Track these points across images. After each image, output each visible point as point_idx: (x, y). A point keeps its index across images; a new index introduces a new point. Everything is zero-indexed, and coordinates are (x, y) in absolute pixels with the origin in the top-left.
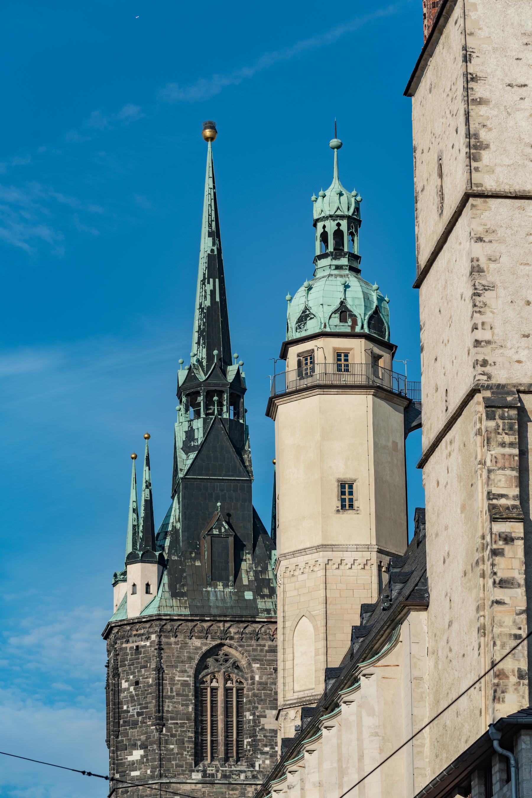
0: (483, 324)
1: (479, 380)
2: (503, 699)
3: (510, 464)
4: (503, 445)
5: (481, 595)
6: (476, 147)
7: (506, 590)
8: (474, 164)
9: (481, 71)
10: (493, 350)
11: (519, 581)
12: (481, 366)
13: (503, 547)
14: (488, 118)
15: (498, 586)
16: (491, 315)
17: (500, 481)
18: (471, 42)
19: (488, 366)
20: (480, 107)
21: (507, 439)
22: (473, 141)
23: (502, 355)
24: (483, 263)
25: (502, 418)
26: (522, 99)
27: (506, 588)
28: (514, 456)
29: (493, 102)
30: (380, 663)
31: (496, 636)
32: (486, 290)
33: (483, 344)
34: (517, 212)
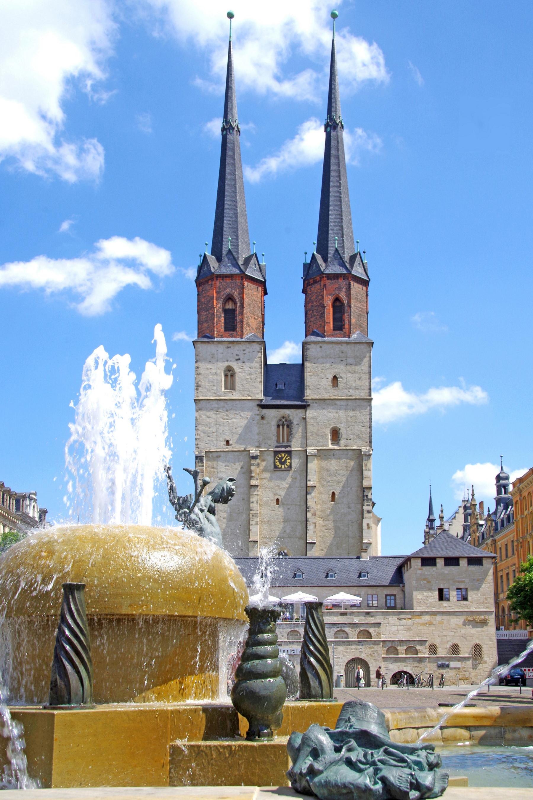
4: (200, 466)
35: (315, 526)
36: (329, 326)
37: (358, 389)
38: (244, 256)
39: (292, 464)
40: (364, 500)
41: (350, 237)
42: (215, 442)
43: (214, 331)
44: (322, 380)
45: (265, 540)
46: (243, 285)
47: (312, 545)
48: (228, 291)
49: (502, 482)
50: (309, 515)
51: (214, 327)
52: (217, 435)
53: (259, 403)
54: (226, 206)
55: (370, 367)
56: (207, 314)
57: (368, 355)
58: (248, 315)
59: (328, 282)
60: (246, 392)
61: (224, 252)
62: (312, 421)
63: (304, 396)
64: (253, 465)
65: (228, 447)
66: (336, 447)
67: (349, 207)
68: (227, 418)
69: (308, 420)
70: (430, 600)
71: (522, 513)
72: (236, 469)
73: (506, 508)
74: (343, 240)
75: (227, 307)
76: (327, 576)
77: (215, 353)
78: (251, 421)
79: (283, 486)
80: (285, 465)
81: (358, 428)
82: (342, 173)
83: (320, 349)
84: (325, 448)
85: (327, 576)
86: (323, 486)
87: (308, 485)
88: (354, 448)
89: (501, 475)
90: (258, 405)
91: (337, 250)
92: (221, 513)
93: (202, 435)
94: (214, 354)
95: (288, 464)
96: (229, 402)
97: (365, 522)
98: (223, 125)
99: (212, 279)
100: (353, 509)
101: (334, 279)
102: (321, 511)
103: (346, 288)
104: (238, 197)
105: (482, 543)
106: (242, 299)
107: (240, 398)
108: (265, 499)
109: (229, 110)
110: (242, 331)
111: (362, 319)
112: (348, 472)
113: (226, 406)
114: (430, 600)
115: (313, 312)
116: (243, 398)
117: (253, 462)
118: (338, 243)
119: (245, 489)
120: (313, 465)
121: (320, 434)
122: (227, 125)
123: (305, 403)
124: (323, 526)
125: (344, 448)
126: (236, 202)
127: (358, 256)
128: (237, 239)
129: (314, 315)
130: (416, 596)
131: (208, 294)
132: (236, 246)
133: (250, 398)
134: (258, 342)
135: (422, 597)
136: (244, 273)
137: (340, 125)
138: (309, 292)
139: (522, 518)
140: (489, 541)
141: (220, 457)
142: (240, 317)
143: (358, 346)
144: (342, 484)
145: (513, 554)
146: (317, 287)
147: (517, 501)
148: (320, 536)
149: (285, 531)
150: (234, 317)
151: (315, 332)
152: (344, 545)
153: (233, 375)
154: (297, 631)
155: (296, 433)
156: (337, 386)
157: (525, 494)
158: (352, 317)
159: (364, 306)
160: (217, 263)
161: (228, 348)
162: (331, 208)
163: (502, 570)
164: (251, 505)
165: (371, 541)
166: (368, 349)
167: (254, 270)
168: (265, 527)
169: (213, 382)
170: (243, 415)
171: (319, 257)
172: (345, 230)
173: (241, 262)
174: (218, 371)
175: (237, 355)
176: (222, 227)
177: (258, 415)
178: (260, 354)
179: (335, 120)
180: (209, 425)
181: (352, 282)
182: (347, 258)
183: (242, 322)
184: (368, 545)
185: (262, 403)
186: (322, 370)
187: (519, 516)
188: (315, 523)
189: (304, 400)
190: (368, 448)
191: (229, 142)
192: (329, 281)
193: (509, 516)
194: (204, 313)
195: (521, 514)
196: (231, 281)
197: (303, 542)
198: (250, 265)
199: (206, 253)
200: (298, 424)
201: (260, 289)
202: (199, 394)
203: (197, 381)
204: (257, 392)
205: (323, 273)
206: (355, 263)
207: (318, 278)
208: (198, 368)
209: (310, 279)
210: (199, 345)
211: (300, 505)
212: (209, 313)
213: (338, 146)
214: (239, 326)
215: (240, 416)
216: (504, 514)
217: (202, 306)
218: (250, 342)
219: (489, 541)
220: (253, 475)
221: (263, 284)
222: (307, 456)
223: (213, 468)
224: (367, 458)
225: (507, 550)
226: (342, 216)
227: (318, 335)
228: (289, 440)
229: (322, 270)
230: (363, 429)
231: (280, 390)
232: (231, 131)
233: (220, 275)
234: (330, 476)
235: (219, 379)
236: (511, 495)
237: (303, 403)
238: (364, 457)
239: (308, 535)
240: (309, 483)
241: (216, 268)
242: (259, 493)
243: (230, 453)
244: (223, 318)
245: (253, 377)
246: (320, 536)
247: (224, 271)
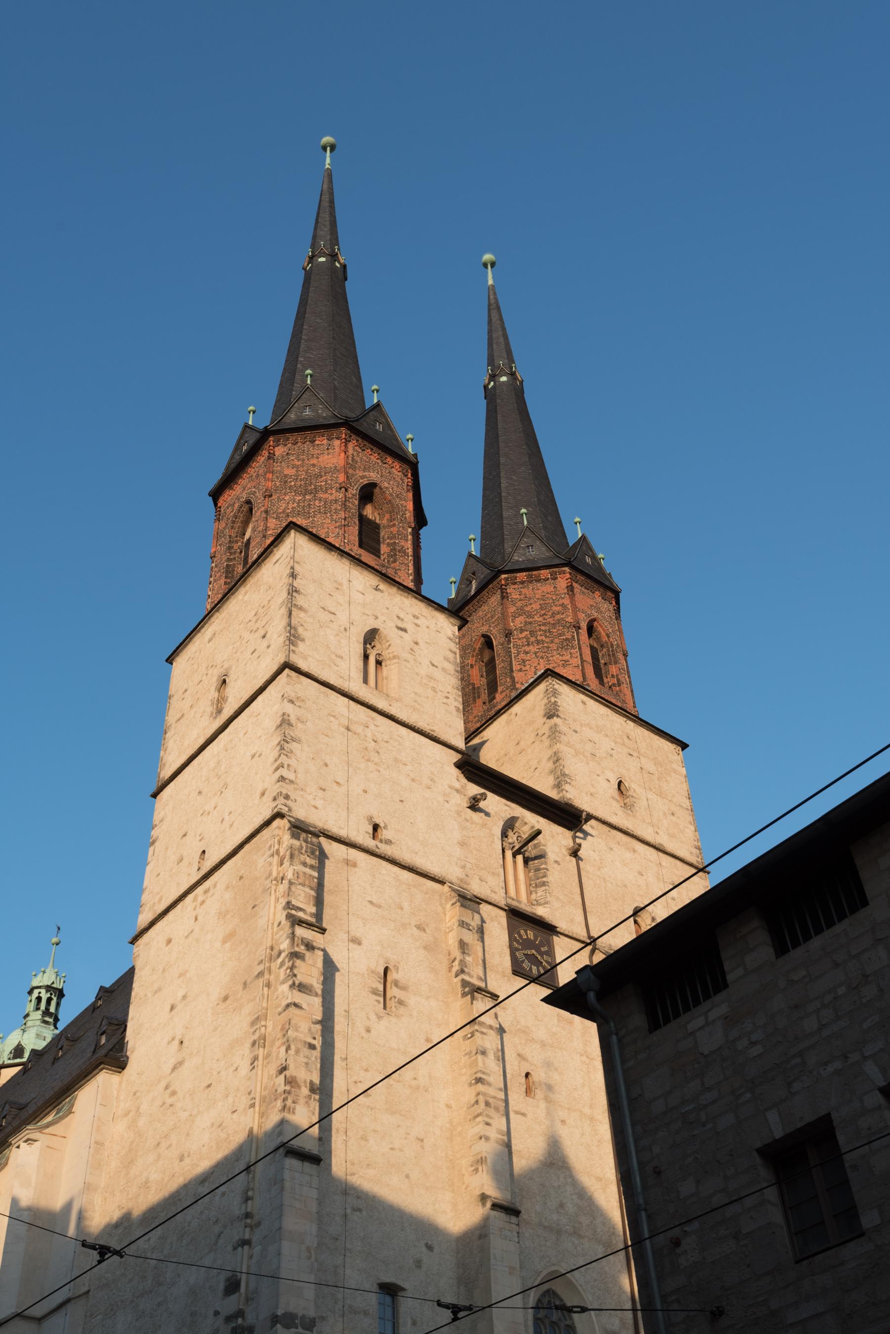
0: (289, 765)
1: (281, 809)
2: (294, 1109)
3: (310, 883)
4: (305, 864)
5: (265, 1005)
6: (294, 636)
7: (304, 995)
8: (292, 647)
9: (303, 589)
10: (295, 789)
11: (317, 990)
12: (284, 798)
13: (304, 952)
14: (305, 622)
15: (297, 988)
16: (295, 761)
17: (300, 895)
18: (297, 568)
19: (290, 801)
20: (300, 612)
21: (309, 861)
22: (292, 631)
23: (302, 796)
24: (293, 719)
25: (306, 841)
26: (331, 621)
27: (304, 993)
28: (314, 877)
29: (310, 613)
30: (47, 1131)
31: (291, 1039)
32: (293, 741)
33: (287, 781)
34: (322, 695)
48: (374, 476)
77: (345, 583)
94: (341, 584)
113: (372, 727)
129: (538, 642)
131: (315, 461)
141: (355, 865)
161: (376, 589)
175: (398, 617)
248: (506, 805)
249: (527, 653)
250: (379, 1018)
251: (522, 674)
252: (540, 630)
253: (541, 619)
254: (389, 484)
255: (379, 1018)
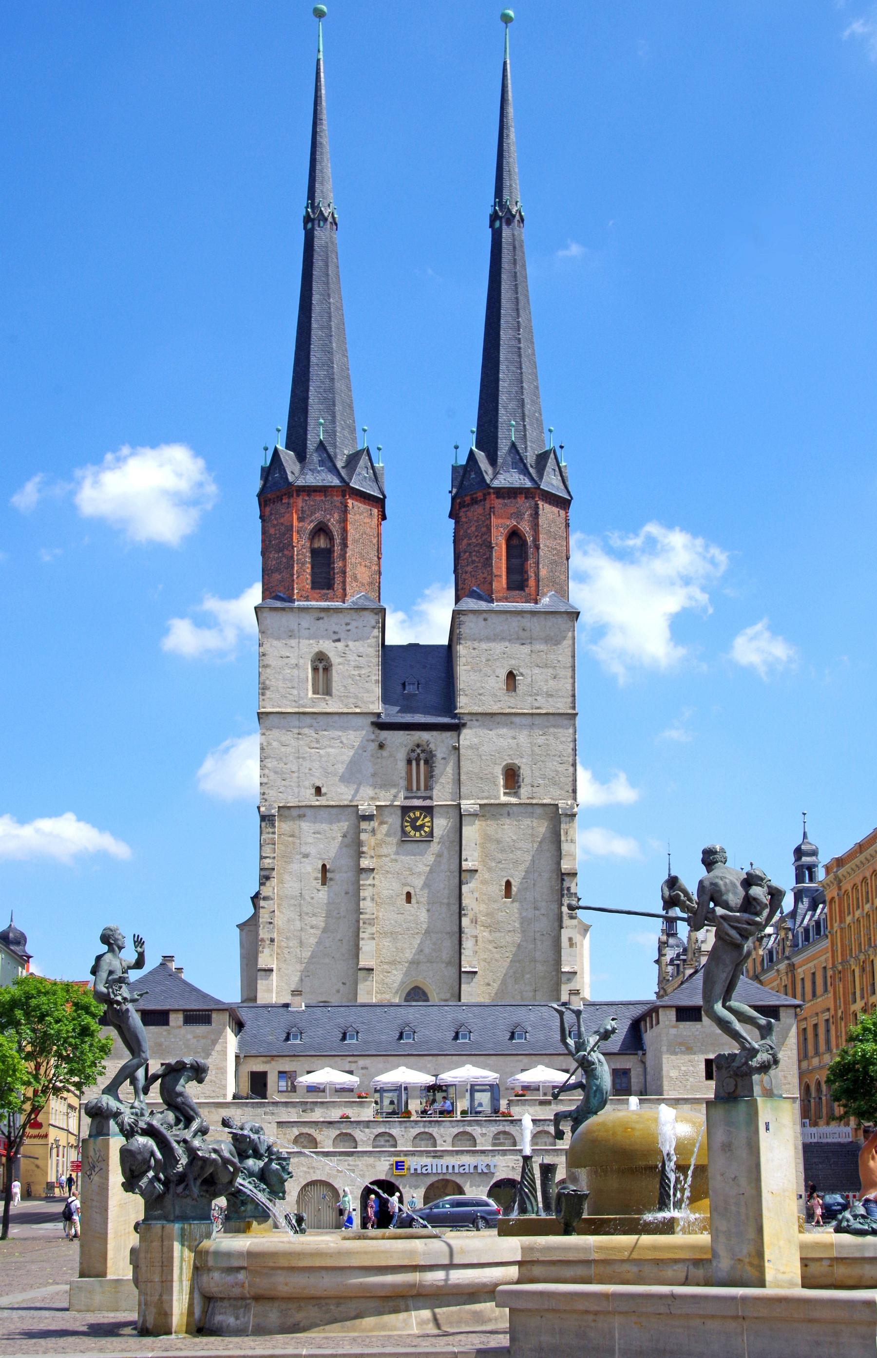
4: (269, 833)
35: (477, 941)
36: (501, 582)
37: (551, 696)
38: (346, 452)
39: (435, 830)
40: (562, 896)
41: (537, 419)
42: (296, 790)
43: (293, 589)
44: (486, 678)
45: (385, 966)
46: (346, 506)
47: (470, 975)
48: (318, 515)
49: (805, 859)
50: (465, 921)
51: (293, 581)
52: (298, 778)
53: (374, 719)
54: (313, 360)
55: (573, 657)
56: (278, 558)
57: (570, 634)
58: (353, 560)
59: (498, 503)
60: (353, 701)
61: (311, 445)
62: (470, 752)
63: (456, 708)
64: (365, 831)
65: (319, 798)
66: (514, 800)
67: (534, 365)
68: (318, 746)
69: (462, 751)
70: (691, 1079)
71: (842, 920)
72: (334, 839)
73: (813, 907)
74: (524, 426)
75: (316, 546)
76: (512, 1037)
77: (296, 627)
78: (360, 751)
79: (418, 870)
80: (422, 832)
81: (552, 766)
82: (521, 305)
83: (483, 622)
84: (492, 801)
85: (512, 1037)
86: (490, 869)
87: (464, 867)
88: (545, 801)
89: (803, 847)
90: (373, 723)
91: (513, 445)
92: (306, 917)
93: (272, 776)
94: (292, 631)
95: (427, 829)
96: (321, 718)
97: (565, 934)
98: (307, 212)
99: (290, 496)
100: (543, 911)
101: (509, 498)
102: (487, 915)
103: (531, 515)
104: (334, 345)
105: (770, 969)
106: (344, 530)
107: (340, 711)
108: (385, 893)
109: (317, 185)
110: (344, 590)
111: (558, 568)
112: (536, 845)
113: (315, 724)
114: (691, 1079)
115: (470, 556)
116: (345, 710)
117: (364, 825)
118: (516, 431)
119: (350, 874)
120: (471, 832)
121: (486, 777)
122: (313, 212)
123: (457, 721)
124: (490, 942)
125: (528, 801)
126: (330, 353)
127: (552, 456)
128: (333, 421)
129: (473, 562)
130: (668, 1072)
131: (282, 520)
132: (332, 433)
133: (358, 710)
134: (372, 610)
135: (677, 1074)
136: (348, 484)
137: (518, 217)
138: (464, 520)
139: (841, 929)
140: (782, 966)
141: (304, 816)
142: (340, 564)
143: (552, 620)
144: (523, 867)
145: (826, 990)
146: (478, 510)
147: (833, 898)
148: (485, 960)
149: (421, 951)
150: (329, 565)
151: (474, 591)
152: (528, 976)
153: (327, 669)
154: (468, 1133)
155: (442, 774)
156: (515, 691)
157: (847, 886)
158: (541, 566)
159: (562, 546)
160: (298, 463)
162: (502, 367)
163: (806, 1019)
164: (361, 902)
165: (576, 968)
166: (570, 624)
167: (365, 477)
168: (386, 942)
169: (291, 681)
170: (345, 741)
171: (480, 456)
172: (528, 407)
173: (340, 464)
174: (301, 661)
175: (334, 632)
176: (306, 399)
177: (373, 741)
178: (376, 631)
179: (508, 209)
180: (284, 759)
181: (540, 503)
182: (530, 459)
183: (344, 572)
184: (570, 976)
185: (381, 720)
186: (488, 660)
187: (836, 925)
188: (476, 937)
189: (456, 714)
190: (569, 802)
191: (317, 243)
192: (500, 501)
193: (818, 923)
194: (273, 555)
195: (841, 922)
196: (323, 498)
197: (453, 971)
198: (358, 470)
199: (278, 446)
200: (444, 758)
201: (375, 511)
202: (266, 703)
203: (263, 678)
204: (371, 699)
205: (488, 486)
206: (547, 469)
207: (480, 495)
208: (264, 655)
209: (466, 495)
210: (266, 614)
211: (448, 904)
212: (284, 555)
213: (515, 255)
214: (338, 579)
215: (341, 742)
216: (810, 920)
217: (270, 541)
218: (359, 610)
219: (782, 966)
220: (365, 849)
221: (379, 503)
222: (461, 816)
223: (292, 836)
224: (568, 819)
225: (814, 983)
226: (522, 382)
227: (479, 597)
228: (429, 787)
229: (488, 481)
230: (561, 768)
231: (412, 696)
232: (322, 223)
233: (304, 486)
234: (503, 851)
235: (302, 676)
236: (823, 886)
237: (453, 721)
238: (563, 819)
239: (463, 957)
240: (465, 865)
241: (297, 475)
242: (376, 882)
243: (322, 808)
244: (309, 566)
245: (363, 672)
246: (485, 960)
247: (311, 479)
248: (408, 735)
249: (466, 573)
250: (318, 890)
251: (463, 591)
252: (474, 551)
253: (474, 541)
254: (331, 515)
255: (318, 890)
